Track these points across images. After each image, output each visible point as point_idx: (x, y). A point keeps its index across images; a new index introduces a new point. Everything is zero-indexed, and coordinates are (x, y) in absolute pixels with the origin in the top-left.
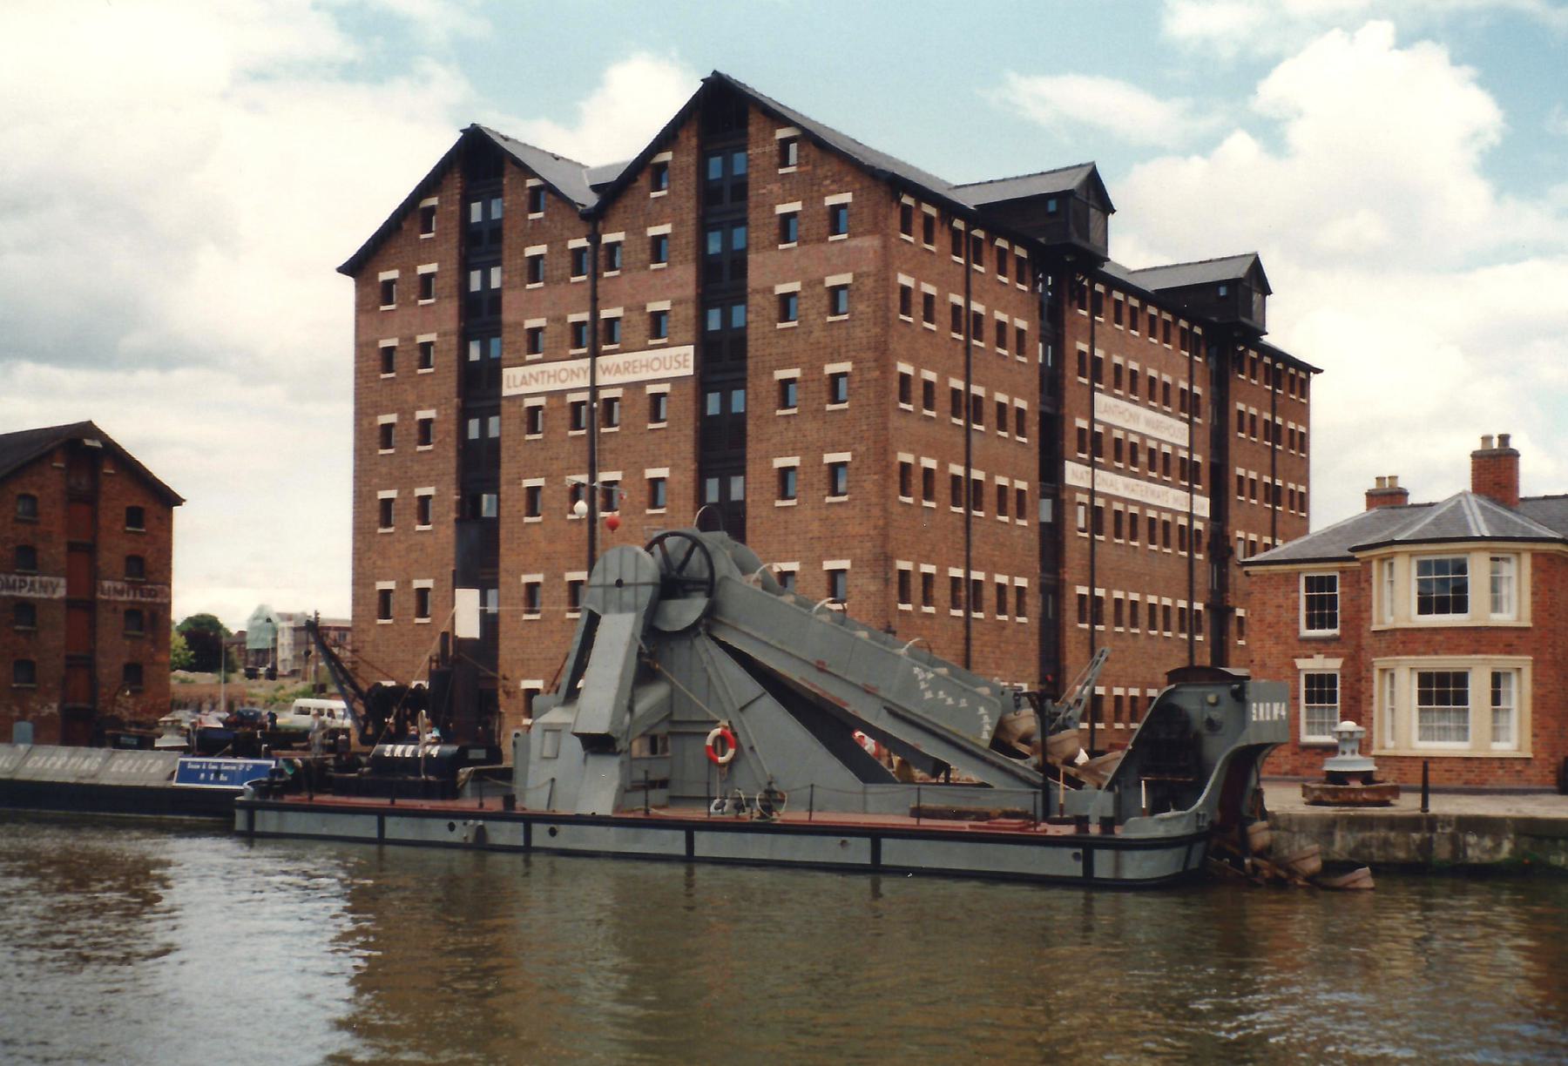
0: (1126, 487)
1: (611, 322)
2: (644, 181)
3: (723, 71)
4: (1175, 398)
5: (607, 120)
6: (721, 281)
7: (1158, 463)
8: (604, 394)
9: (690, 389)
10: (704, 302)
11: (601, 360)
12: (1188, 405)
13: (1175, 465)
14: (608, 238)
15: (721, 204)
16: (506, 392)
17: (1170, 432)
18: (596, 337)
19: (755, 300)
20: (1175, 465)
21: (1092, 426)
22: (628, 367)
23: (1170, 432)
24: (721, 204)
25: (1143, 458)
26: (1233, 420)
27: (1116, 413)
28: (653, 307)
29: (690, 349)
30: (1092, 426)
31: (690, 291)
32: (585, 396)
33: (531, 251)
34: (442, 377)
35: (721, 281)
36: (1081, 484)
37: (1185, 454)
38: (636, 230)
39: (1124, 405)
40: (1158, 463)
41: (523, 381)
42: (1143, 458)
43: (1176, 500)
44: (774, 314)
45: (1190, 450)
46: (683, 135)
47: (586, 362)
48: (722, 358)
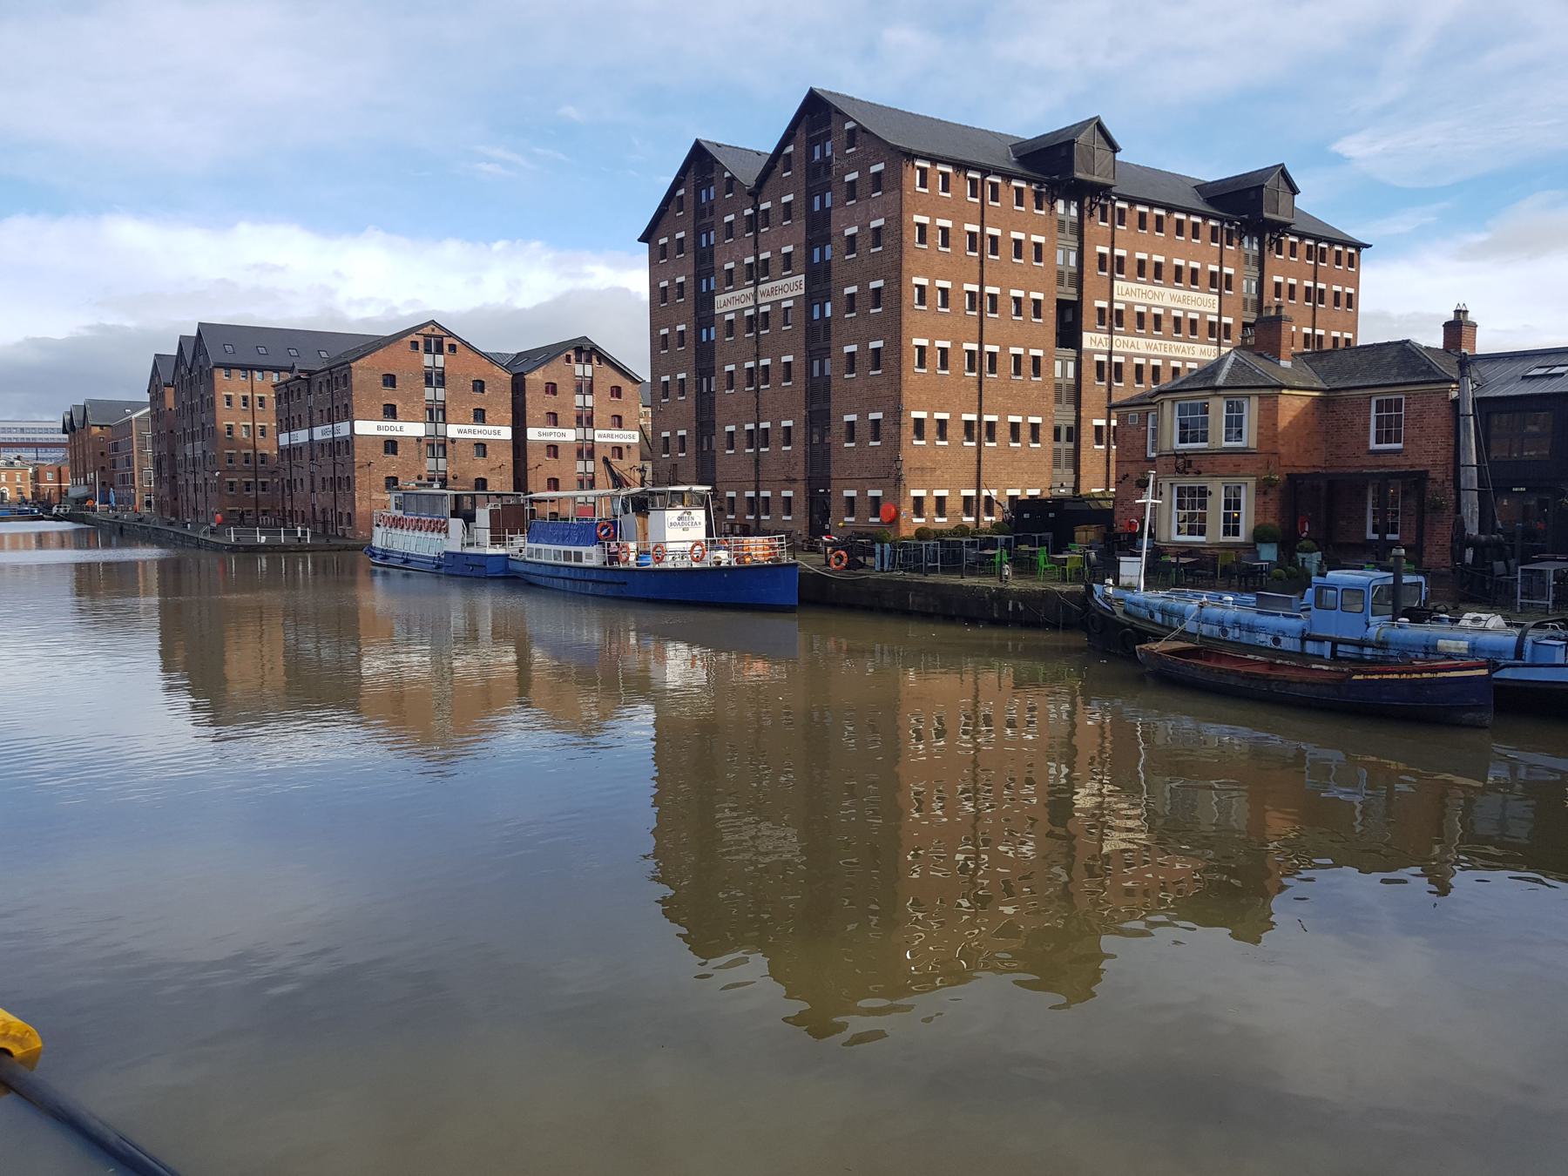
0: (1148, 346)
1: (766, 261)
2: (780, 165)
3: (817, 86)
4: (1204, 279)
5: (755, 130)
6: (818, 229)
7: (1184, 327)
8: (762, 309)
9: (802, 301)
10: (809, 246)
11: (761, 288)
12: (1219, 282)
13: (1203, 328)
14: (764, 206)
15: (818, 176)
16: (717, 311)
17: (1203, 304)
18: (758, 272)
19: (835, 240)
20: (1203, 328)
21: (1111, 305)
22: (773, 291)
23: (1203, 304)
24: (818, 176)
25: (1167, 325)
26: (1269, 290)
27: (1130, 293)
28: (785, 250)
29: (802, 277)
30: (1111, 305)
31: (803, 239)
32: (751, 312)
33: (727, 219)
34: (686, 303)
35: (818, 229)
36: (1100, 347)
37: (1215, 319)
38: (776, 200)
39: (1134, 286)
40: (1184, 327)
41: (729, 303)
42: (1167, 325)
43: (1202, 352)
44: (844, 248)
45: (1220, 315)
46: (798, 133)
47: (752, 290)
48: (819, 281)
